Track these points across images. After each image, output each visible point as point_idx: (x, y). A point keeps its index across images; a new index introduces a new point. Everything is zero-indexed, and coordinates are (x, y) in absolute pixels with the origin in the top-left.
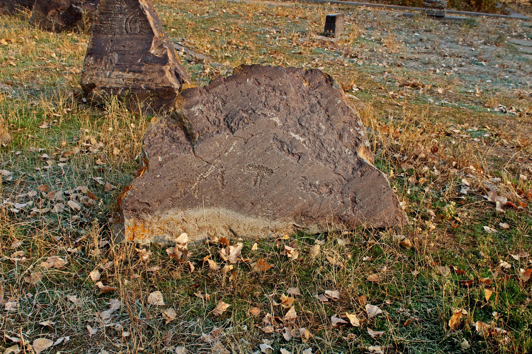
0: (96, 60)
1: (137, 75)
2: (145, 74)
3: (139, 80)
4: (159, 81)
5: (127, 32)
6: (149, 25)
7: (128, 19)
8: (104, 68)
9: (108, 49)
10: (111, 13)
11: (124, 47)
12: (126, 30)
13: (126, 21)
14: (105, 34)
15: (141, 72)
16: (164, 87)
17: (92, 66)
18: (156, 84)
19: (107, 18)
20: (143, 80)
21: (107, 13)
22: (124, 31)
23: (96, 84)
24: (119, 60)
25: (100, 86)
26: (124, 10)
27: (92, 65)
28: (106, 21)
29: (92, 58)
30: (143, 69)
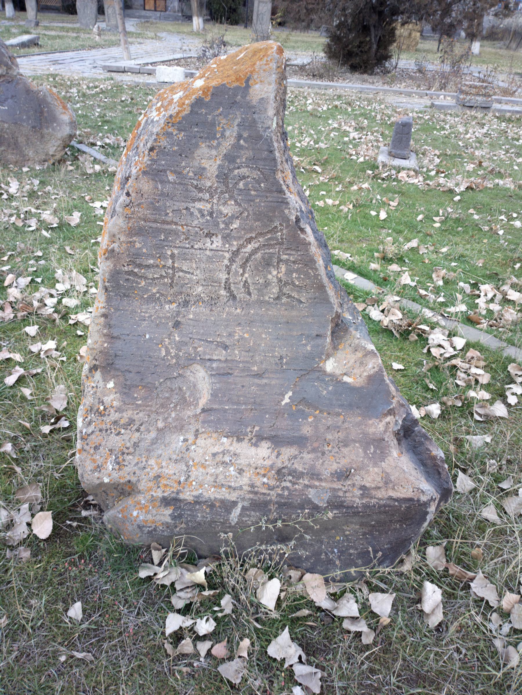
0: (126, 390)
1: (288, 452)
2: (314, 450)
3: (300, 475)
4: (371, 477)
5: (233, 297)
6: (316, 276)
7: (236, 253)
9: (168, 352)
10: (176, 233)
11: (226, 347)
12: (227, 288)
13: (232, 260)
14: (152, 299)
15: (300, 442)
16: (391, 498)
17: (114, 416)
18: (363, 488)
19: (159, 247)
20: (315, 475)
21: (159, 231)
22: (223, 292)
23: (142, 486)
24: (214, 395)
25: (159, 494)
26: (227, 224)
27: (119, 410)
28: (153, 257)
29: (111, 385)
30: (306, 430)
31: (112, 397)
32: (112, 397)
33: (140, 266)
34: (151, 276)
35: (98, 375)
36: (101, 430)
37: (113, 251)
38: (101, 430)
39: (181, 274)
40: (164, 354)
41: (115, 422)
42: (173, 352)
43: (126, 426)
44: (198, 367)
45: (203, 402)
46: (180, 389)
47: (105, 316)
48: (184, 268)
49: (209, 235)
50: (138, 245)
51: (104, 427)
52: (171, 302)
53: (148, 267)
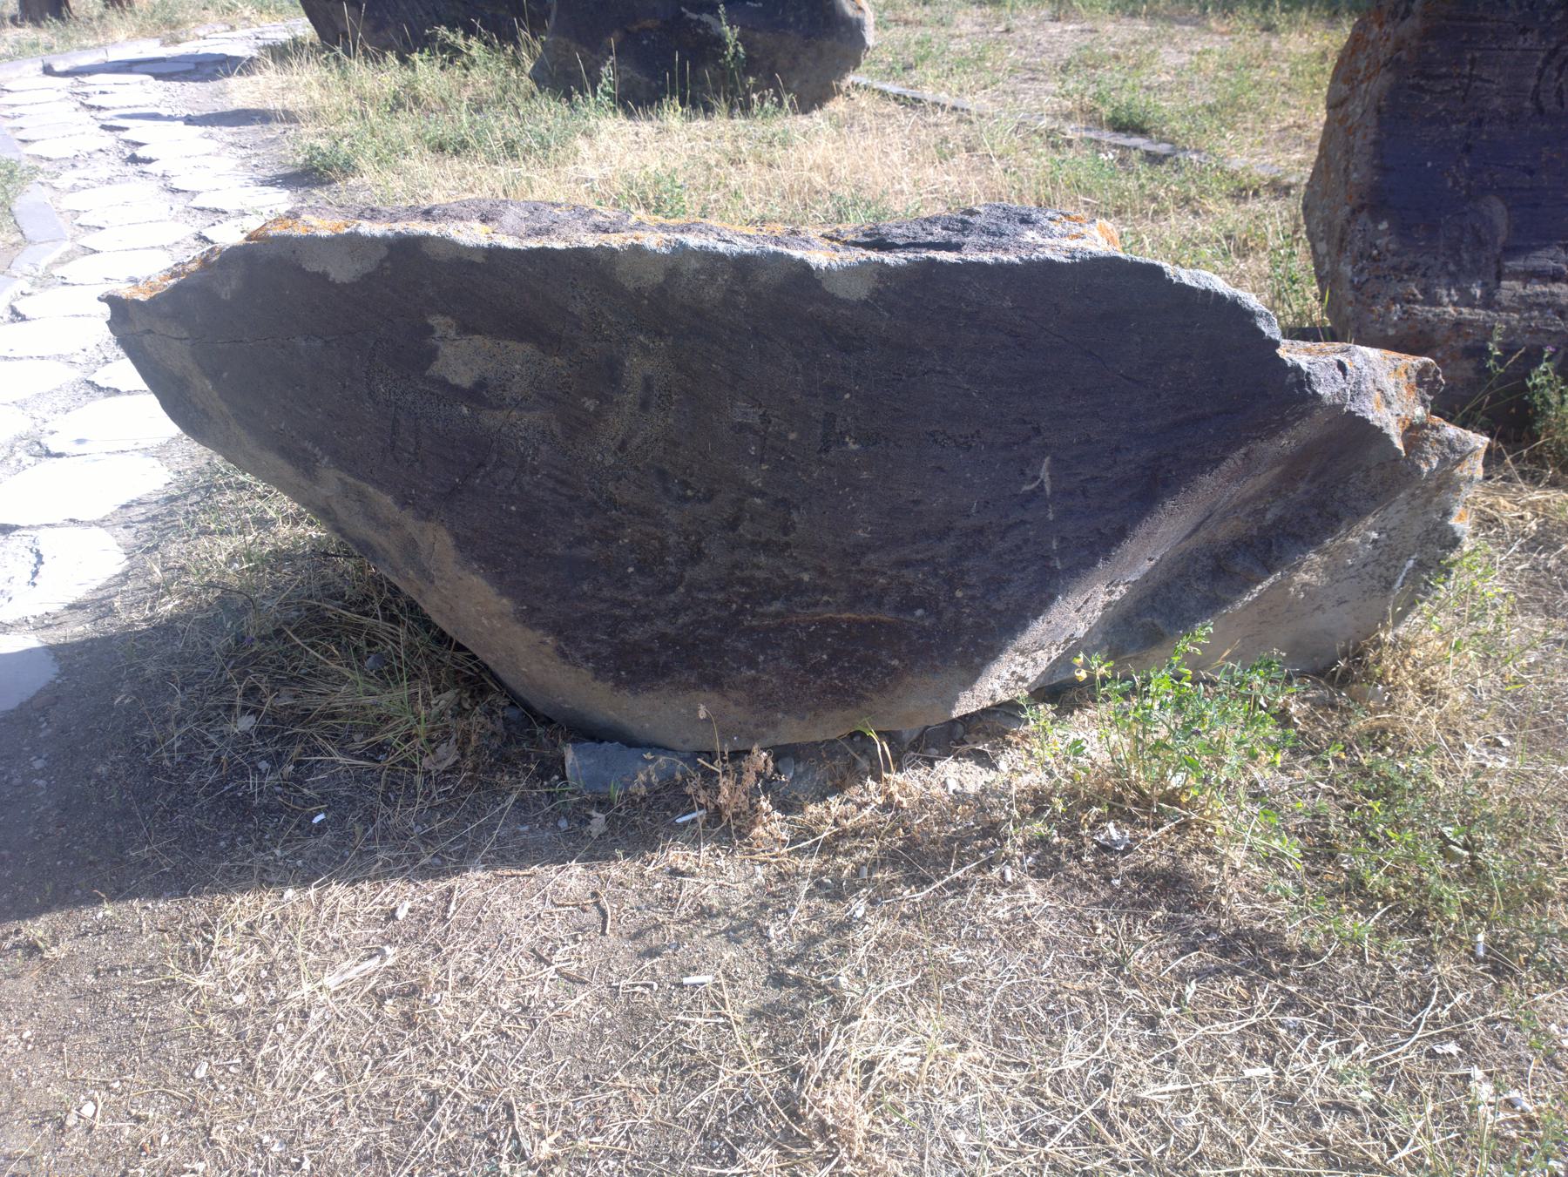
8: (1452, 267)
9: (1456, 182)
11: (1531, 173)
31: (1386, 239)
32: (1386, 239)
33: (1428, 77)
34: (1439, 89)
35: (1364, 216)
36: (1377, 277)
37: (1399, 59)
38: (1377, 277)
39: (1478, 83)
40: (1450, 184)
41: (1394, 268)
42: (1463, 181)
43: (1409, 270)
44: (1493, 199)
45: (1501, 239)
46: (1473, 227)
47: (1374, 143)
48: (1484, 75)
49: (1524, 31)
50: (1431, 50)
51: (1381, 273)
52: (1458, 121)
53: (1439, 77)
